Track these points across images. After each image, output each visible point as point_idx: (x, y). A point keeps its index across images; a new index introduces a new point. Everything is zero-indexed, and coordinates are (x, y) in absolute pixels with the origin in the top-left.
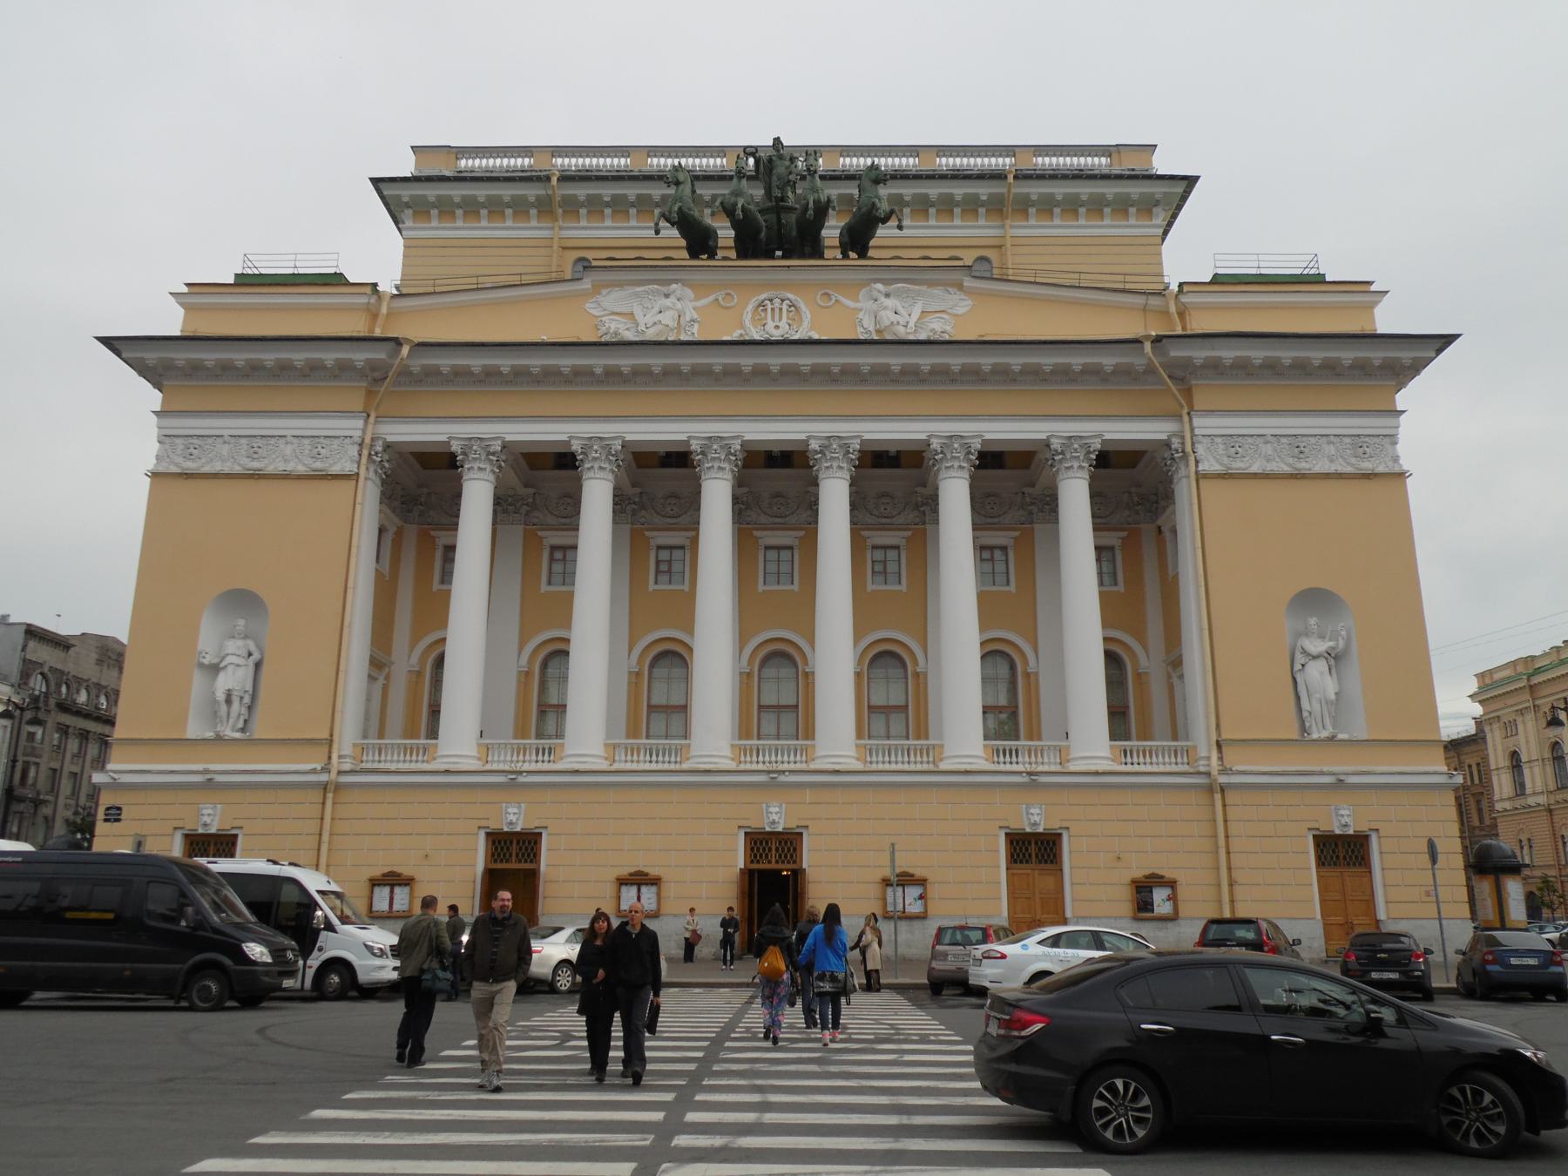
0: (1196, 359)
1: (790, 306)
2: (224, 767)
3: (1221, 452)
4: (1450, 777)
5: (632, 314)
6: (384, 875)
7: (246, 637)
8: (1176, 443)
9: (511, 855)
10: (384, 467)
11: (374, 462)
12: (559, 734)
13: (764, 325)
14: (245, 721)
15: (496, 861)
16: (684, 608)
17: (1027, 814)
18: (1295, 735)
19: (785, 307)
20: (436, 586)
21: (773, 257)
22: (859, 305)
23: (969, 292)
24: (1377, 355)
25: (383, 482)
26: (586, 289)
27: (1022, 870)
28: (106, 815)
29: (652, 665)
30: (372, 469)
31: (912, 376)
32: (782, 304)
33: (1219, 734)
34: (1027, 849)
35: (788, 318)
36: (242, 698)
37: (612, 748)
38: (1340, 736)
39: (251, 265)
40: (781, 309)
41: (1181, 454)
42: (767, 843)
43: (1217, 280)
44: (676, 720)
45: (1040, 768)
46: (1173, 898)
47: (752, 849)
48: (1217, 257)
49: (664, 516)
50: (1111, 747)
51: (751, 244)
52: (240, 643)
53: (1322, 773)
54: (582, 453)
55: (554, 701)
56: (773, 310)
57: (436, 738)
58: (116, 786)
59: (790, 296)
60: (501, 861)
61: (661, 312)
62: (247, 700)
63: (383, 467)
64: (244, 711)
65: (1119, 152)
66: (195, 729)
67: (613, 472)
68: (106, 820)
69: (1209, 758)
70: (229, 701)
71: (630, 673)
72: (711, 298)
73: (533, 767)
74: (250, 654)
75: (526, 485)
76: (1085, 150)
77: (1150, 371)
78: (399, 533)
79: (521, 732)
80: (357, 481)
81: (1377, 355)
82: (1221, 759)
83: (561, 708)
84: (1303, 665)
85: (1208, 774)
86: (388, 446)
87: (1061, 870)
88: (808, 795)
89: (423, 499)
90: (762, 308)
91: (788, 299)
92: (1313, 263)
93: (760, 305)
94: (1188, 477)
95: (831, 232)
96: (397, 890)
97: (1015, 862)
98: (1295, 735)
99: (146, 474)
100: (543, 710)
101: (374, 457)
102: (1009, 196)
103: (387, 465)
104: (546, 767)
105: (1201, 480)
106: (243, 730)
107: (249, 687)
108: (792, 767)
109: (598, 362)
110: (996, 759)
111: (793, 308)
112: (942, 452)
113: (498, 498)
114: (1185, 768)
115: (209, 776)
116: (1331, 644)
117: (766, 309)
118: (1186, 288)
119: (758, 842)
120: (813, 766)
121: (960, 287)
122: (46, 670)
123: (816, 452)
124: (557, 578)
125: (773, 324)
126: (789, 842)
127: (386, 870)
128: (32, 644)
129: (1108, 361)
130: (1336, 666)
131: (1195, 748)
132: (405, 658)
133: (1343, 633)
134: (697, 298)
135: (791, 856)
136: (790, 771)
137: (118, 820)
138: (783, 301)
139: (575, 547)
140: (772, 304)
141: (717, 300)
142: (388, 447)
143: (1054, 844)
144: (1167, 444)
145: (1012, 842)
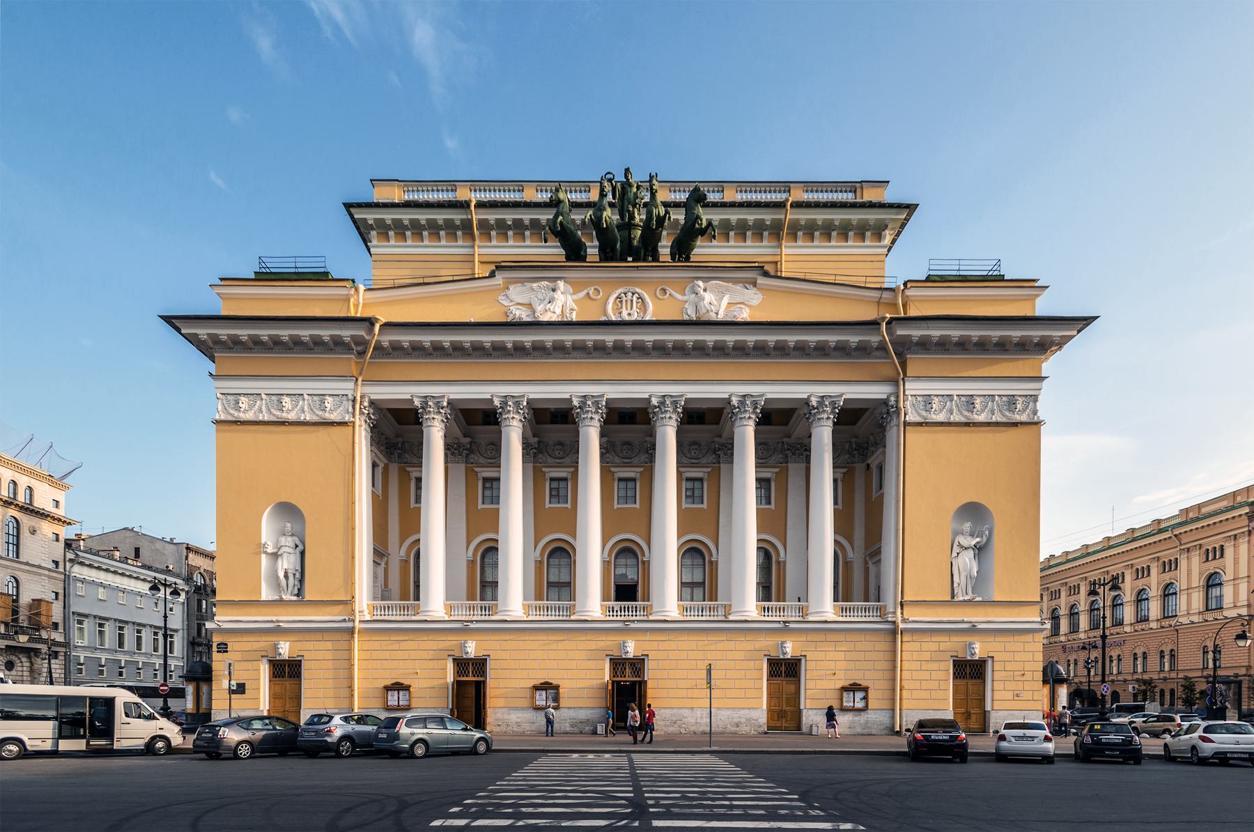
0: (914, 337)
1: (638, 299)
2: (287, 618)
3: (922, 407)
4: (1042, 625)
5: (531, 304)
6: (392, 684)
7: (293, 535)
8: (892, 399)
9: (469, 672)
10: (371, 418)
11: (363, 413)
12: (495, 598)
13: (620, 313)
14: (299, 589)
15: (460, 676)
16: (570, 520)
17: (782, 647)
18: (949, 599)
19: (635, 299)
20: (413, 505)
21: (626, 261)
22: (685, 298)
23: (762, 289)
24: (1036, 333)
25: (372, 429)
26: (498, 285)
27: (777, 681)
28: (218, 648)
29: (549, 556)
30: (363, 418)
31: (720, 350)
32: (632, 297)
33: (902, 598)
34: (779, 669)
35: (637, 307)
36: (294, 575)
37: (527, 608)
38: (977, 599)
39: (265, 266)
40: (632, 301)
41: (895, 409)
42: (623, 665)
43: (929, 279)
44: (565, 591)
45: (790, 619)
46: (865, 698)
47: (614, 669)
48: (932, 262)
49: (554, 458)
50: (834, 606)
51: (608, 253)
52: (290, 539)
53: (963, 622)
54: (501, 407)
55: (490, 579)
56: (626, 301)
57: (419, 600)
58: (221, 631)
59: (638, 290)
60: (463, 676)
61: (550, 302)
62: (298, 575)
63: (370, 418)
64: (297, 583)
65: (862, 188)
66: (266, 594)
67: (521, 420)
68: (218, 652)
69: (895, 613)
70: (286, 576)
71: (536, 561)
72: (585, 292)
73: (479, 618)
74: (297, 546)
75: (465, 436)
76: (838, 186)
77: (882, 347)
78: (386, 469)
79: (471, 597)
80: (354, 427)
81: (1036, 333)
82: (902, 613)
83: (495, 584)
84: (958, 554)
85: (894, 622)
86: (372, 403)
87: (799, 681)
88: (648, 637)
89: (400, 446)
90: (619, 299)
91: (637, 293)
92: (996, 267)
93: (617, 298)
94: (898, 426)
95: (665, 248)
96: (401, 693)
97: (772, 676)
98: (949, 599)
99: (212, 422)
100: (484, 584)
101: (364, 410)
102: (785, 221)
103: (372, 417)
104: (487, 618)
105: (907, 427)
106: (298, 595)
107: (298, 567)
108: (638, 618)
109: (509, 338)
110: (763, 614)
111: (640, 300)
112: (738, 407)
113: (448, 445)
114: (878, 619)
115: (277, 624)
116: (978, 540)
117: (622, 301)
118: (909, 285)
119: (618, 664)
120: (651, 618)
121: (755, 284)
122: (202, 571)
123: (656, 407)
124: (487, 500)
125: (628, 312)
126: (637, 664)
127: (394, 681)
128: (191, 555)
129: (853, 339)
130: (978, 554)
131: (885, 606)
132: (397, 552)
133: (987, 532)
134: (574, 293)
135: (638, 673)
136: (637, 621)
137: (227, 652)
138: (633, 294)
139: (498, 479)
140: (626, 297)
141: (588, 294)
142: (372, 403)
143: (796, 665)
144: (885, 402)
145: (770, 665)
